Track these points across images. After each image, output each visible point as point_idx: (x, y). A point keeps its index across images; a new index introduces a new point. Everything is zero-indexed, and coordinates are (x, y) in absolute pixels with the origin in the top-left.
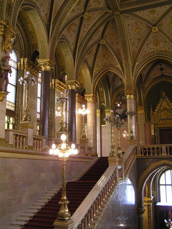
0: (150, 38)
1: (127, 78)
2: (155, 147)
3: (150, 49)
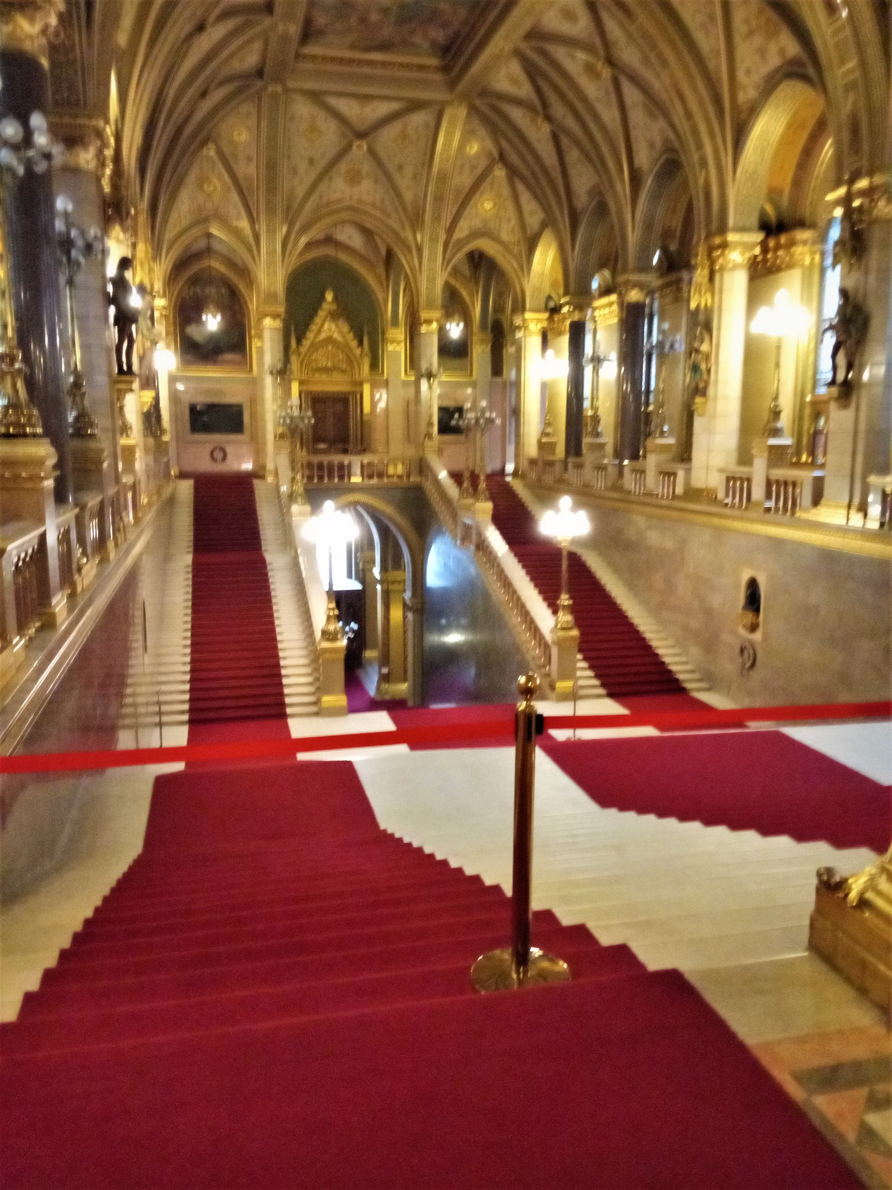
0: (343, 166)
1: (268, 267)
2: (336, 463)
3: (335, 192)
